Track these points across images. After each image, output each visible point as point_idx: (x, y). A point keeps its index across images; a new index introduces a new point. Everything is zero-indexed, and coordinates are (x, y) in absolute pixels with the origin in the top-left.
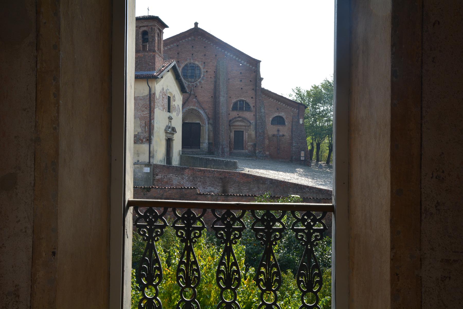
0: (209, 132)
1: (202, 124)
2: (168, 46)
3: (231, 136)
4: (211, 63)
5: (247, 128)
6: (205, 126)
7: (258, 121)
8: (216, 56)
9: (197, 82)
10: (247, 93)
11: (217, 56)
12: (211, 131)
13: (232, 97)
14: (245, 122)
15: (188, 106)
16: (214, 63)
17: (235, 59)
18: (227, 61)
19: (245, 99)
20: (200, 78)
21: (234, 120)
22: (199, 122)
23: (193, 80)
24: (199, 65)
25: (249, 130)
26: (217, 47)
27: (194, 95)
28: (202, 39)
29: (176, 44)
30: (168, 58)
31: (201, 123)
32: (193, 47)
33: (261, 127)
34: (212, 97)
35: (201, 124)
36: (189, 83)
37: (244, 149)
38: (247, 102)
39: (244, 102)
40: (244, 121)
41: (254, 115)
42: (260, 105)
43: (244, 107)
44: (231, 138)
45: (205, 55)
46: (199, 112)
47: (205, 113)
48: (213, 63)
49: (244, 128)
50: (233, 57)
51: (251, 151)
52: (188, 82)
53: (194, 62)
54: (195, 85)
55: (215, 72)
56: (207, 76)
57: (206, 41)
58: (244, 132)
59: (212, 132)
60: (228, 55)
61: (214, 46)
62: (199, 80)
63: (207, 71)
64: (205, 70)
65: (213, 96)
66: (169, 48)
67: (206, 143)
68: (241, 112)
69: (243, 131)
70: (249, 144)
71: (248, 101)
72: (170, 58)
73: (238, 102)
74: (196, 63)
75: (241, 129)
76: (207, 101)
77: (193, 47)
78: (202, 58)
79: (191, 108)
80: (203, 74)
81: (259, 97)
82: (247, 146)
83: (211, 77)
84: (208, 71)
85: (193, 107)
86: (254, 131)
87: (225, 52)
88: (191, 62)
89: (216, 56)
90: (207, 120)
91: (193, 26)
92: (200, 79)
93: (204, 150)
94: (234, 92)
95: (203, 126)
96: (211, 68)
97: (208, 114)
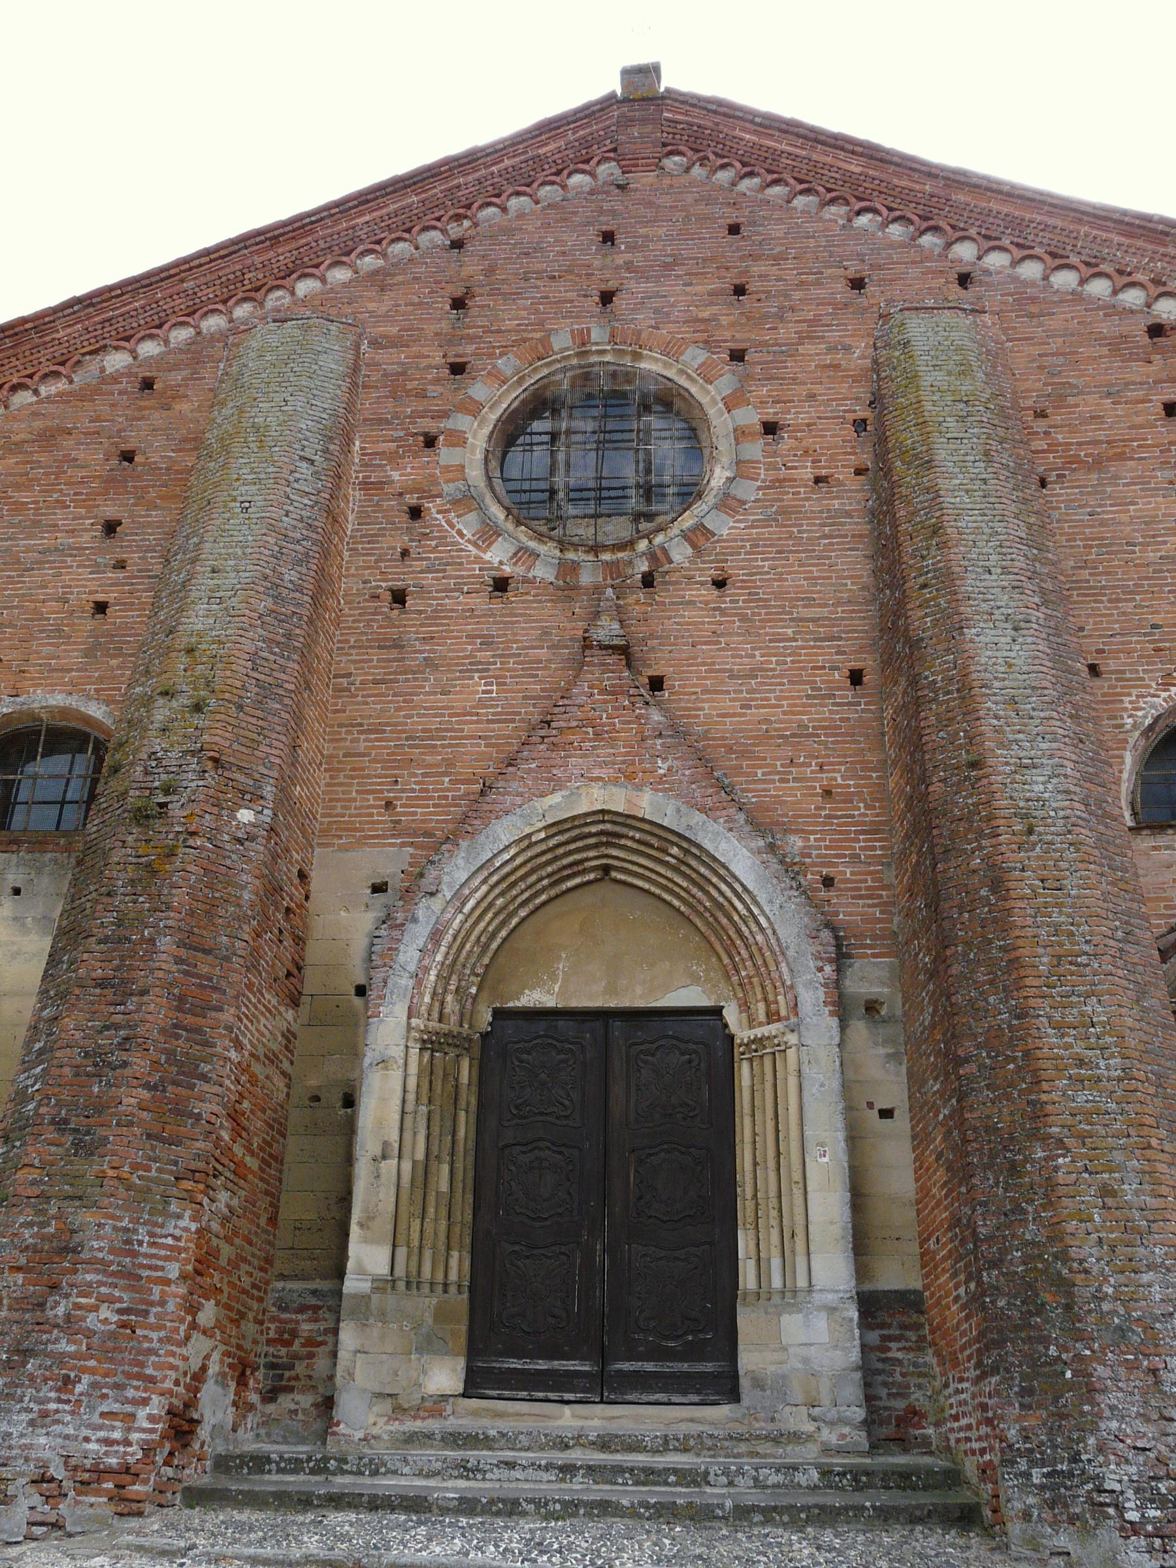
0: (854, 1139)
1: (752, 1023)
2: (363, 254)
4: (808, 348)
6: (792, 1039)
8: (857, 284)
9: (659, 539)
11: (870, 289)
12: (886, 1114)
15: (557, 785)
16: (847, 349)
17: (1076, 297)
18: (987, 318)
20: (700, 496)
22: (704, 1001)
23: (617, 529)
24: (683, 381)
26: (864, 220)
27: (614, 648)
28: (697, 171)
29: (444, 232)
30: (357, 347)
31: (732, 1015)
32: (608, 237)
34: (856, 678)
35: (734, 1027)
36: (571, 555)
45: (740, 290)
46: (690, 846)
47: (791, 869)
48: (832, 349)
50: (1046, 278)
52: (563, 546)
53: (627, 361)
54: (644, 566)
55: (860, 425)
56: (771, 467)
57: (746, 185)
59: (902, 1123)
60: (987, 272)
61: (833, 209)
62: (687, 521)
63: (770, 428)
64: (750, 417)
65: (869, 663)
66: (376, 272)
67: (817, 1298)
72: (375, 343)
74: (644, 365)
76: (802, 726)
77: (608, 237)
78: (714, 318)
79: (583, 808)
80: (725, 460)
83: (818, 480)
84: (789, 419)
85: (617, 800)
87: (949, 245)
88: (595, 359)
89: (857, 284)
90: (817, 957)
91: (614, 85)
92: (699, 508)
93: (796, 1420)
94: (1129, 607)
95: (759, 1041)
96: (819, 390)
97: (828, 882)
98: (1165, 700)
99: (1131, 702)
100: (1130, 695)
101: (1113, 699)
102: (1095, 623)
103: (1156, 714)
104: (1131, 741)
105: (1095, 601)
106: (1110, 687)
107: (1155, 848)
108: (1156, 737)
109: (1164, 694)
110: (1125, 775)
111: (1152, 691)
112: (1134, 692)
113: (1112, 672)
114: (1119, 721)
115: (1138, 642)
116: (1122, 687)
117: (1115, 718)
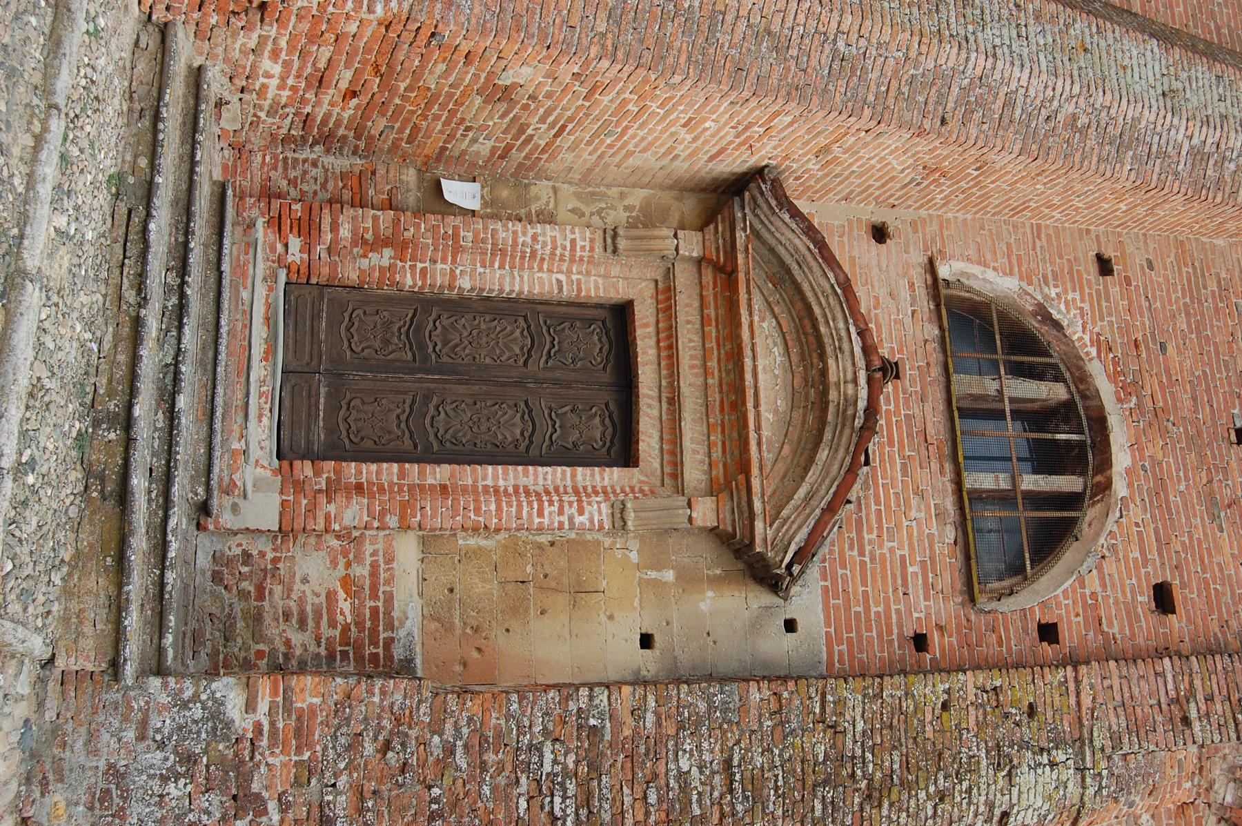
3: (550, 232)
5: (705, 512)
7: (852, 695)
10: (1214, 517)
13: (1115, 290)
14: (811, 460)
19: (1120, 488)
21: (815, 281)
25: (659, 567)
33: (755, 783)
37: (305, 469)
38: (1091, 513)
39: (1067, 483)
40: (823, 455)
41: (920, 642)
42: (1097, 744)
43: (1004, 483)
44: (504, 232)
49: (694, 474)
51: (257, 618)
58: (614, 476)
68: (935, 421)
69: (626, 455)
70: (408, 550)
71: (1110, 525)
73: (1056, 392)
75: (674, 401)
81: (1210, 699)
82: (352, 513)
86: (648, 662)
94: (1182, 323)
98: (1080, 339)
99: (1074, 300)
100: (1082, 301)
101: (1077, 283)
102: (1159, 284)
103: (1065, 324)
104: (1030, 289)
105: (1183, 290)
106: (1089, 281)
107: (912, 285)
108: (1034, 324)
109: (1087, 338)
110: (990, 275)
111: (1089, 327)
112: (1086, 306)
113: (1106, 287)
114: (1051, 283)
115: (1143, 324)
116: (1090, 295)
117: (1055, 279)
